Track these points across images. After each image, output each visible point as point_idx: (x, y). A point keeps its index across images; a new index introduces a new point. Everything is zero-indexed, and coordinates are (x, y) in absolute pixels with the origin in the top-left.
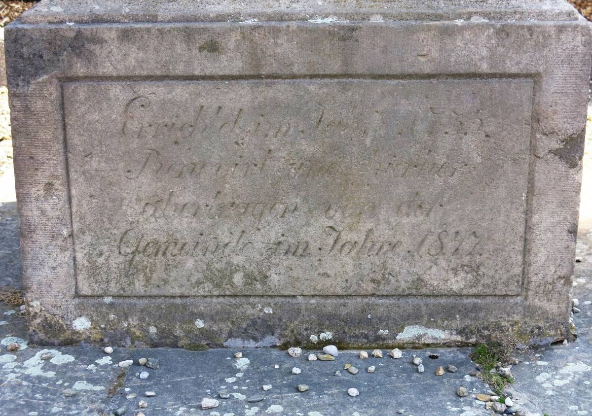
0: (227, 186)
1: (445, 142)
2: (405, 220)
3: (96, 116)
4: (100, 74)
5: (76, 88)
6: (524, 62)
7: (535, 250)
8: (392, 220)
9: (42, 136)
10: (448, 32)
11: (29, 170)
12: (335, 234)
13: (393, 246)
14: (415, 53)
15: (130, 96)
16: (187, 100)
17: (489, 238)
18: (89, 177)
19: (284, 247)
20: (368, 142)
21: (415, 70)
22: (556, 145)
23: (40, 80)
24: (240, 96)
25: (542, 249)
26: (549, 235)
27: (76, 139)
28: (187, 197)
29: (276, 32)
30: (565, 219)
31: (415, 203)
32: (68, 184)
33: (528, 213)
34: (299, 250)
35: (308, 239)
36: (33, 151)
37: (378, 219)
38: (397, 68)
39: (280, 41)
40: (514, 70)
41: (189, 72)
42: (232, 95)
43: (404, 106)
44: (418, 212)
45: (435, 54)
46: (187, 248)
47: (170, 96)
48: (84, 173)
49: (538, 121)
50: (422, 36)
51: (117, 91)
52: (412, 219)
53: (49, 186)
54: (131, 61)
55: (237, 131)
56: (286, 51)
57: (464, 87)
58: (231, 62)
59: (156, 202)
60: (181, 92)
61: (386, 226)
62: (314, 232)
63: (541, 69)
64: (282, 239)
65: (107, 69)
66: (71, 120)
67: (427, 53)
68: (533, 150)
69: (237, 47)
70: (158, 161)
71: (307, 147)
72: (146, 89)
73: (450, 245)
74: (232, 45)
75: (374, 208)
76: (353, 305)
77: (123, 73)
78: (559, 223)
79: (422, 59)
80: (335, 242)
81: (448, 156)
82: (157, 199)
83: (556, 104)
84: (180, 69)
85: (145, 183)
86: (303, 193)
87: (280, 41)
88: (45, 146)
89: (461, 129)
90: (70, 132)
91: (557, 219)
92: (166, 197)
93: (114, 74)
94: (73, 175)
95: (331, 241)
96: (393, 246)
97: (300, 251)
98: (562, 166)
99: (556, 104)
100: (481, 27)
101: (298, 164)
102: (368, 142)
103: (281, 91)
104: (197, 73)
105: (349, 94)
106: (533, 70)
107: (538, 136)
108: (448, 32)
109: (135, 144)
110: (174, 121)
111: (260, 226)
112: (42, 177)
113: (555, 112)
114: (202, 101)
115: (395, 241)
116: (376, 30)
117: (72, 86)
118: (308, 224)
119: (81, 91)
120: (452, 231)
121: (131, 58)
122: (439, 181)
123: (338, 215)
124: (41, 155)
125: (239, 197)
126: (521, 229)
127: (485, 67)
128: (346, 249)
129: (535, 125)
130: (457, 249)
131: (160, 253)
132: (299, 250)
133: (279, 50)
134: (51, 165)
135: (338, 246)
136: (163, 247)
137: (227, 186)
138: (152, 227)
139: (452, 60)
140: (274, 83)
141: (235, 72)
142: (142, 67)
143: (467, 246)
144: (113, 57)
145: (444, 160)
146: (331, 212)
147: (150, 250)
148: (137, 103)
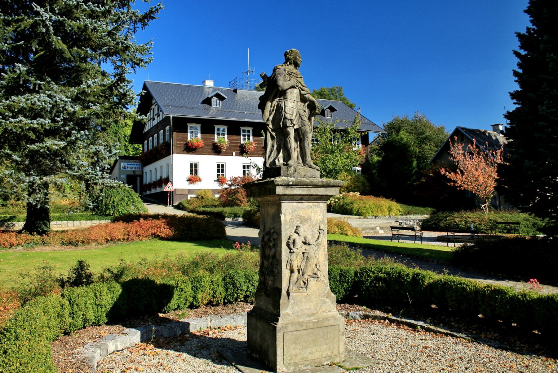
1: (329, 335)
24: (305, 332)
28: (298, 347)
31: (326, 344)
34: (312, 353)
51: (290, 333)
56: (311, 325)
57: (331, 327)
58: (304, 328)
59: (295, 348)
60: (298, 332)
62: (314, 350)
67: (326, 323)
70: (295, 343)
71: (313, 338)
72: (294, 333)
76: (319, 360)
85: (293, 346)
108: (329, 320)
138: (294, 352)
144: (290, 328)
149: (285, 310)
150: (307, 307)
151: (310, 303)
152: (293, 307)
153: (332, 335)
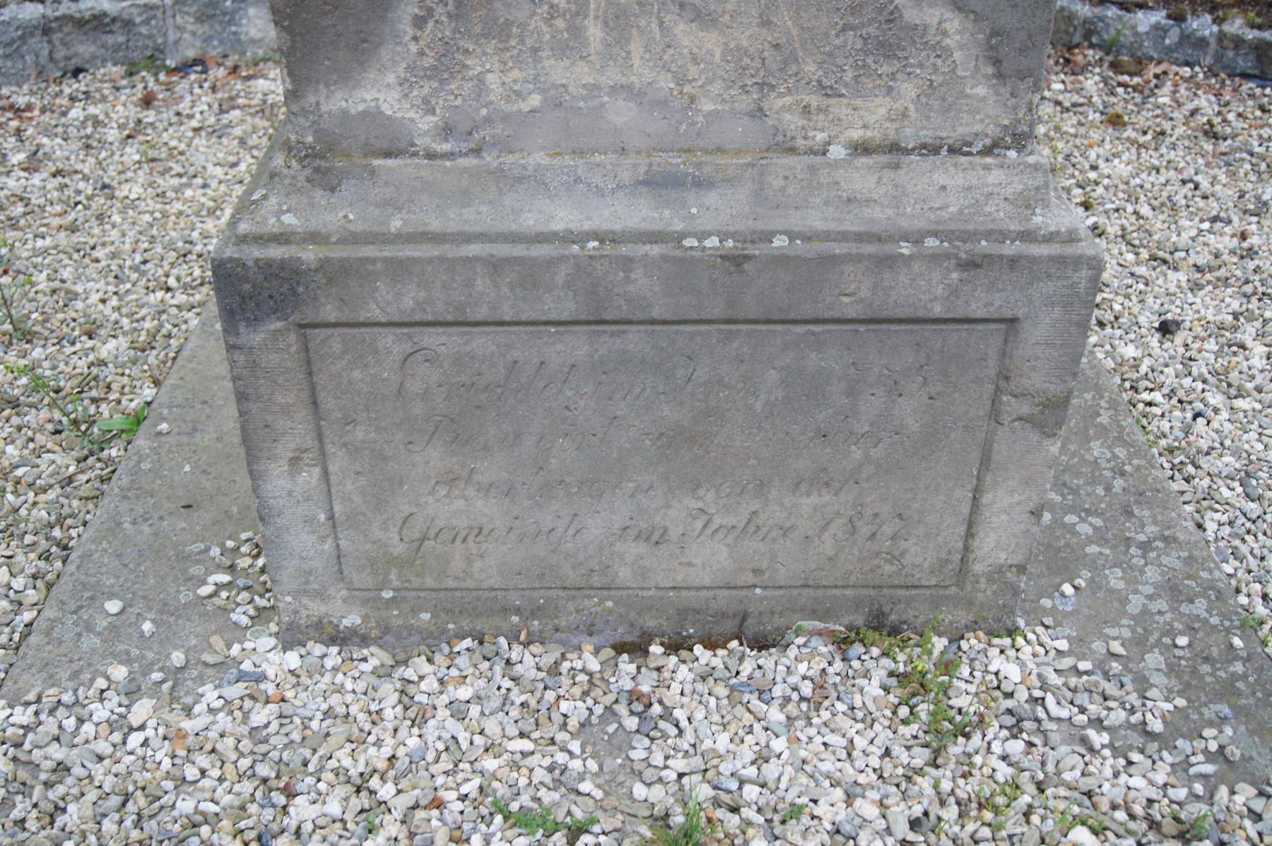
0: (553, 461)
1: (871, 405)
2: (805, 501)
3: (357, 374)
4: (361, 319)
5: (328, 338)
6: (998, 303)
7: (982, 534)
8: (786, 501)
9: (279, 399)
10: (890, 261)
11: (264, 441)
12: (704, 518)
13: (785, 532)
14: (837, 291)
15: (408, 348)
16: (492, 354)
17: (919, 522)
18: (353, 451)
19: (633, 533)
20: (759, 406)
21: (836, 314)
22: (1025, 409)
23: (272, 327)
24: (577, 346)
25: (992, 534)
26: (1004, 517)
27: (328, 403)
29: (627, 263)
30: (1029, 499)
31: (820, 480)
32: (323, 454)
33: (977, 492)
34: (655, 538)
35: (667, 523)
36: (269, 418)
37: (767, 500)
38: (808, 311)
39: (633, 276)
40: (980, 314)
41: (497, 317)
42: (560, 347)
43: (813, 360)
44: (824, 491)
45: (864, 293)
46: (496, 534)
47: (468, 348)
48: (345, 445)
49: (1007, 378)
50: (849, 268)
51: (388, 340)
52: (814, 499)
53: (295, 462)
54: (408, 302)
55: (569, 393)
60: (482, 342)
61: (777, 508)
62: (676, 514)
63: (1020, 314)
64: (629, 523)
65: (375, 313)
66: (321, 379)
67: (854, 292)
68: (995, 414)
69: (568, 285)
71: (668, 413)
72: (430, 338)
73: (864, 530)
74: (560, 278)
75: (761, 487)
77: (396, 319)
78: (1019, 503)
79: (845, 299)
80: (705, 526)
81: (872, 425)
82: (452, 476)
83: (1036, 358)
84: (482, 313)
85: (434, 457)
86: (661, 470)
87: (633, 276)
88: (286, 411)
89: (895, 390)
90: (322, 395)
91: (1017, 498)
92: (465, 473)
93: (383, 320)
94: (330, 449)
95: (698, 525)
96: (785, 532)
97: (655, 537)
98: (1034, 437)
99: (1036, 358)
100: (935, 258)
101: (656, 434)
102: (759, 406)
103: (634, 340)
104: (507, 318)
105: (735, 345)
106: (1008, 314)
107: (1005, 399)
109: (418, 409)
110: (474, 380)
111: (599, 508)
112: (285, 449)
113: (1034, 369)
114: (515, 354)
115: (788, 524)
116: (780, 260)
117: (321, 333)
118: (668, 506)
119: (336, 342)
120: (869, 513)
121: (409, 300)
122: (857, 453)
123: (710, 496)
124: (282, 423)
125: (570, 474)
126: (966, 510)
127: (938, 310)
128: (720, 535)
129: (1003, 384)
130: (874, 534)
131: (459, 540)
132: (655, 538)
133: (631, 288)
134: (295, 433)
135: (709, 531)
136: (463, 533)
137: (553, 461)
139: (891, 300)
140: (624, 332)
141: (565, 316)
142: (424, 311)
143: (888, 529)
145: (867, 428)
146: (701, 492)
147: (445, 536)
148: (419, 357)
149: (346, 76)
150: (641, 72)
151: (685, 34)
152: (445, 66)
153: (909, 412)
